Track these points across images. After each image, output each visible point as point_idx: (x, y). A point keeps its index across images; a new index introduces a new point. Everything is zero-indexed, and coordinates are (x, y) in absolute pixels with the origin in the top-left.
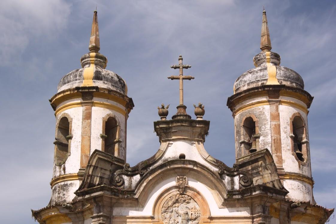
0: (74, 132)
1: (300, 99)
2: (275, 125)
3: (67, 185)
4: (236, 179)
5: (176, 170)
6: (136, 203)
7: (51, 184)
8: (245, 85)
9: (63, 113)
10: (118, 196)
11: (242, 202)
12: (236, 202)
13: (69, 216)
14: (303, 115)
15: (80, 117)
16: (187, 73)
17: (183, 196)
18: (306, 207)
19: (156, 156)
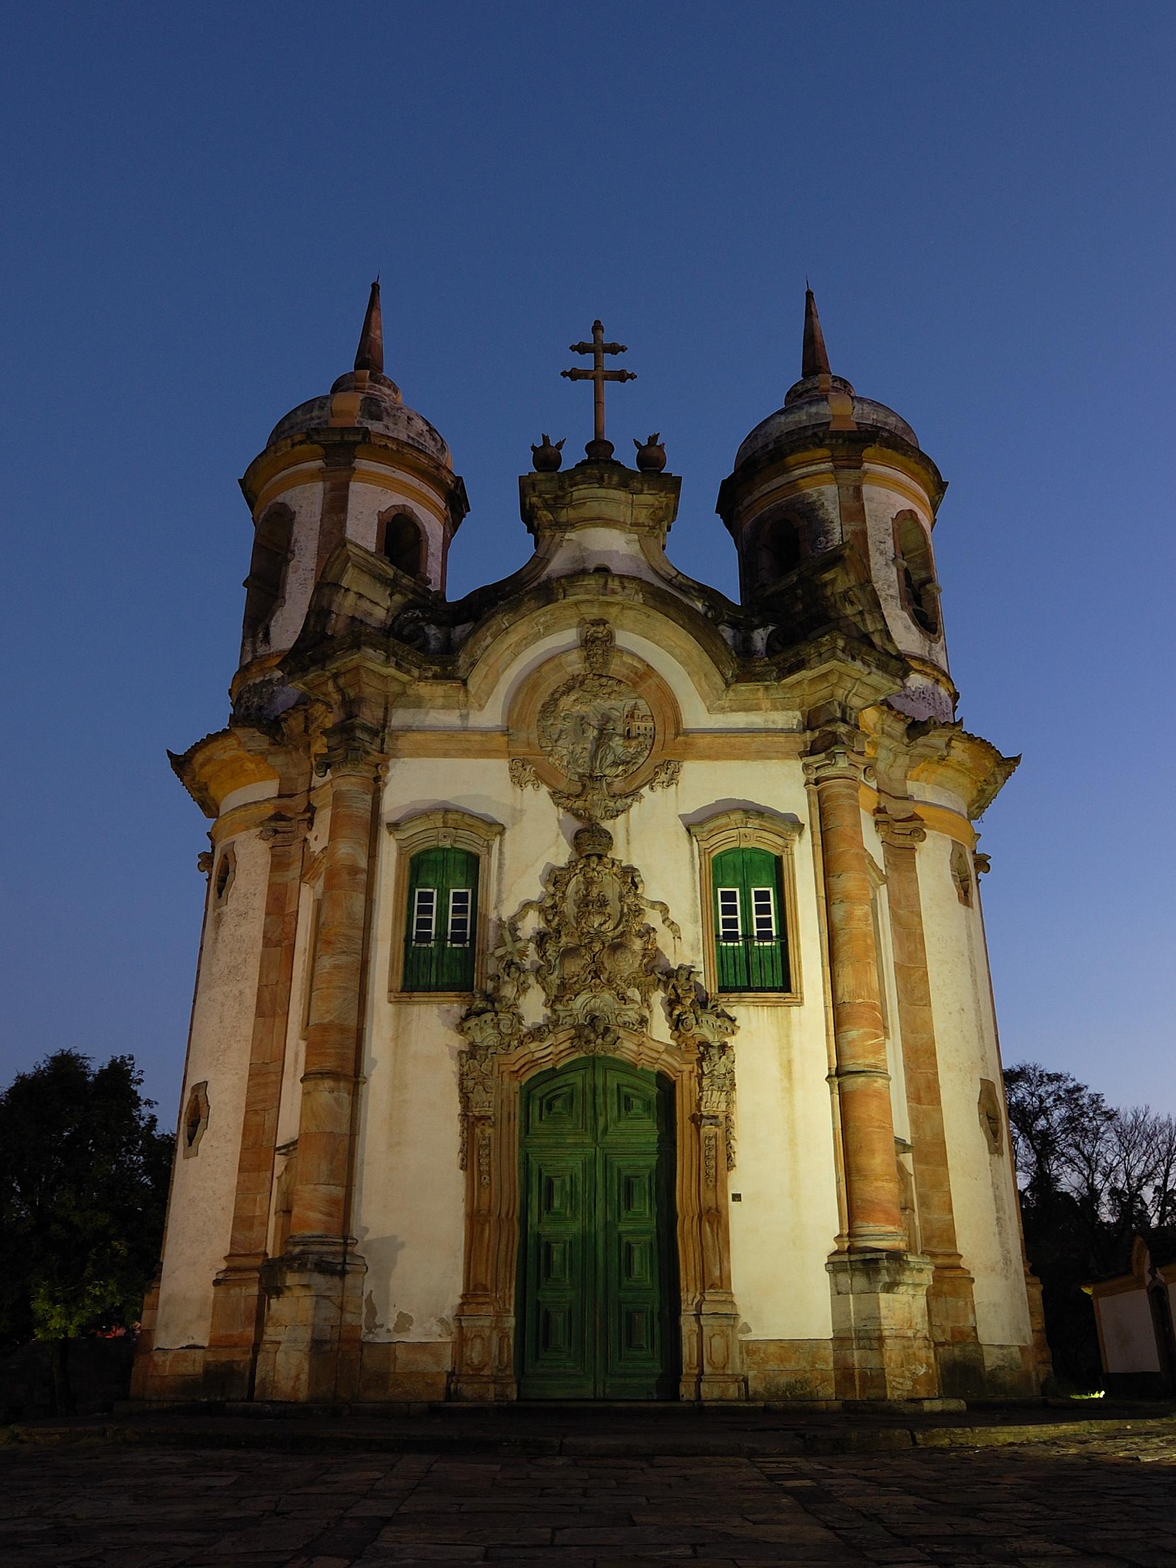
0: (298, 545)
1: (914, 475)
2: (855, 533)
3: (270, 681)
4: (759, 637)
5: (584, 609)
6: (461, 696)
7: (230, 694)
8: (767, 445)
9: (270, 504)
10: (408, 672)
11: (777, 694)
12: (760, 694)
13: (271, 760)
14: (926, 523)
15: (317, 509)
16: (611, 363)
17: (604, 681)
18: (951, 739)
19: (523, 574)
